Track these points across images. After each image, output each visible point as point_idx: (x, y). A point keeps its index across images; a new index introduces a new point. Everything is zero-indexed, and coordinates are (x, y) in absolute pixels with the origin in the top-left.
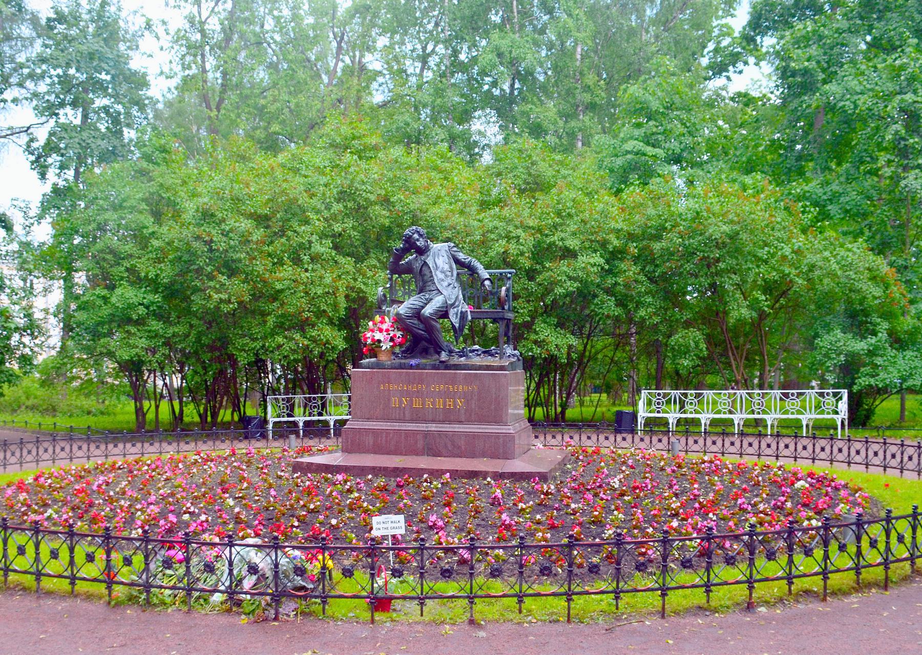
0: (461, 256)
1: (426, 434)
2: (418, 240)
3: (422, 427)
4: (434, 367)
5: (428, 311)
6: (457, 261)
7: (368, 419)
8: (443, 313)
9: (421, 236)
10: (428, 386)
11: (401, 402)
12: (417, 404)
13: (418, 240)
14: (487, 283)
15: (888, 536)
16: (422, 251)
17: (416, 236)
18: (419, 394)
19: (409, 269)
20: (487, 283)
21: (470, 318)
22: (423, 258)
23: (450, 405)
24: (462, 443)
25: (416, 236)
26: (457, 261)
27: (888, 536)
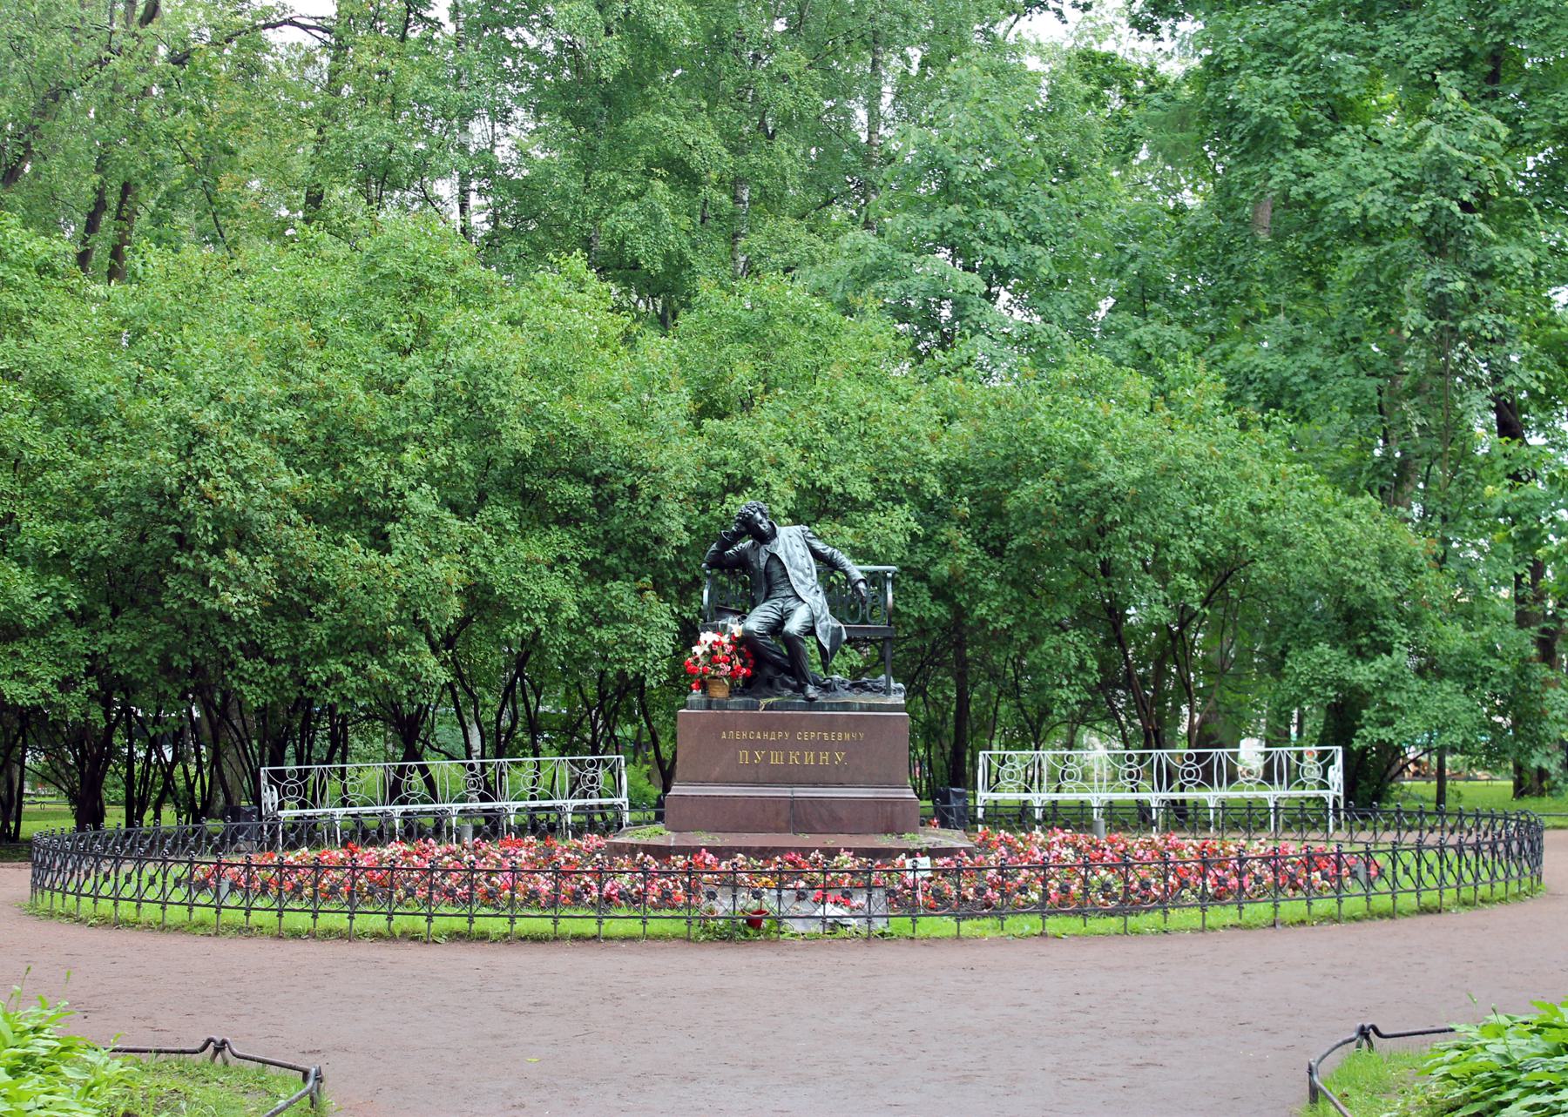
0: (818, 545)
1: (793, 802)
3: (785, 792)
4: (801, 707)
7: (703, 782)
8: (811, 631)
9: (763, 514)
10: (793, 734)
11: (752, 757)
12: (776, 759)
14: (862, 586)
15: (1394, 866)
16: (764, 538)
17: (758, 516)
18: (779, 745)
19: (743, 562)
20: (862, 586)
24: (843, 813)
25: (758, 516)
26: (816, 554)
27: (1394, 866)
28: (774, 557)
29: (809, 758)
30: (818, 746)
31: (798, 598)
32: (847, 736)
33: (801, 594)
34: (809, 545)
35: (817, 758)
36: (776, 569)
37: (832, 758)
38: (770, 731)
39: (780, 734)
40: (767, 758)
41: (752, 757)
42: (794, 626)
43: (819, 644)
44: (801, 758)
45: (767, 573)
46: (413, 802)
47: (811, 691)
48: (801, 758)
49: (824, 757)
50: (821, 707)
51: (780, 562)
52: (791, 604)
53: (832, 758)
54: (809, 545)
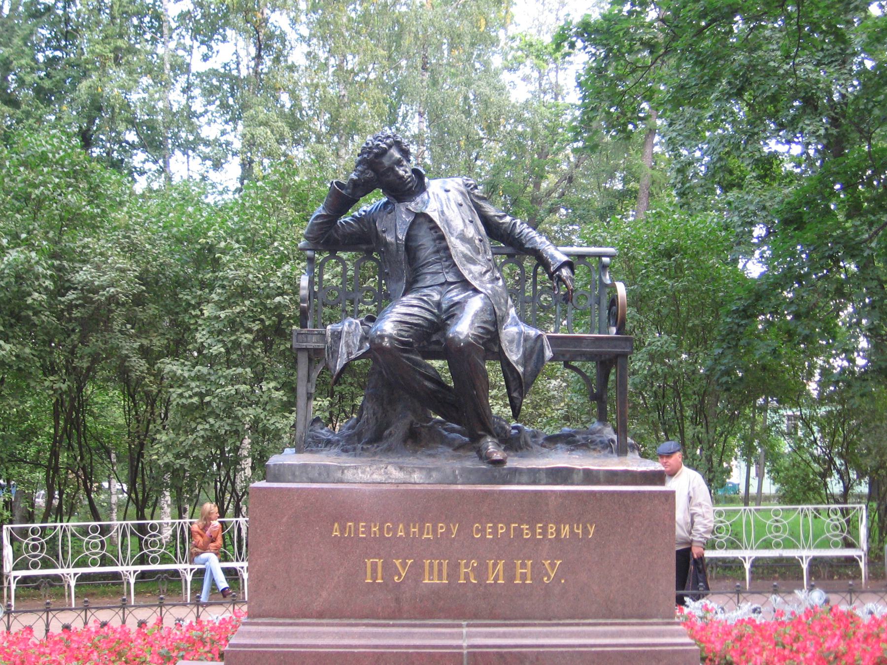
2: (399, 163)
5: (464, 327)
6: (486, 220)
8: (490, 339)
11: (389, 569)
13: (399, 163)
14: (565, 272)
19: (365, 239)
20: (565, 272)
21: (548, 354)
22: (412, 206)
23: (524, 577)
28: (422, 217)
29: (496, 574)
30: (511, 549)
31: (465, 284)
32: (565, 531)
33: (468, 277)
34: (478, 208)
35: (510, 570)
36: (426, 241)
37: (538, 571)
38: (422, 520)
39: (441, 529)
40: (417, 571)
41: (389, 569)
42: (464, 327)
43: (507, 366)
44: (480, 572)
45: (410, 247)
46: (35, 566)
47: (491, 446)
48: (480, 572)
49: (524, 570)
50: (514, 475)
51: (435, 228)
52: (456, 295)
53: (538, 571)
54: (478, 208)
